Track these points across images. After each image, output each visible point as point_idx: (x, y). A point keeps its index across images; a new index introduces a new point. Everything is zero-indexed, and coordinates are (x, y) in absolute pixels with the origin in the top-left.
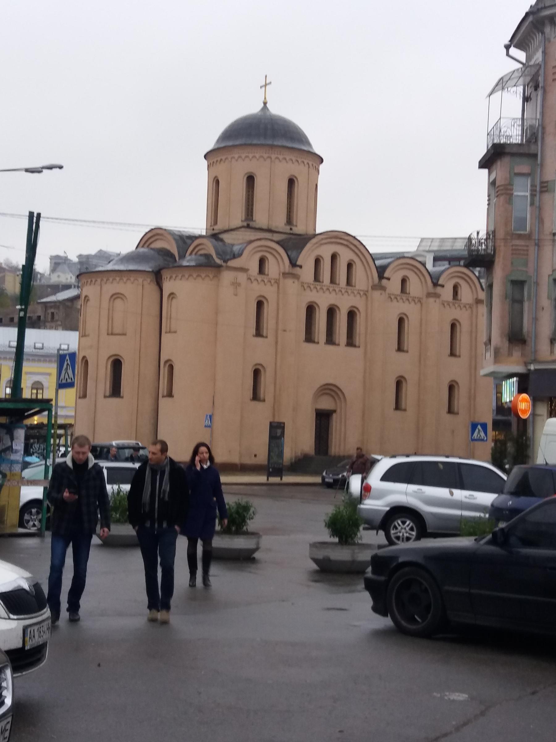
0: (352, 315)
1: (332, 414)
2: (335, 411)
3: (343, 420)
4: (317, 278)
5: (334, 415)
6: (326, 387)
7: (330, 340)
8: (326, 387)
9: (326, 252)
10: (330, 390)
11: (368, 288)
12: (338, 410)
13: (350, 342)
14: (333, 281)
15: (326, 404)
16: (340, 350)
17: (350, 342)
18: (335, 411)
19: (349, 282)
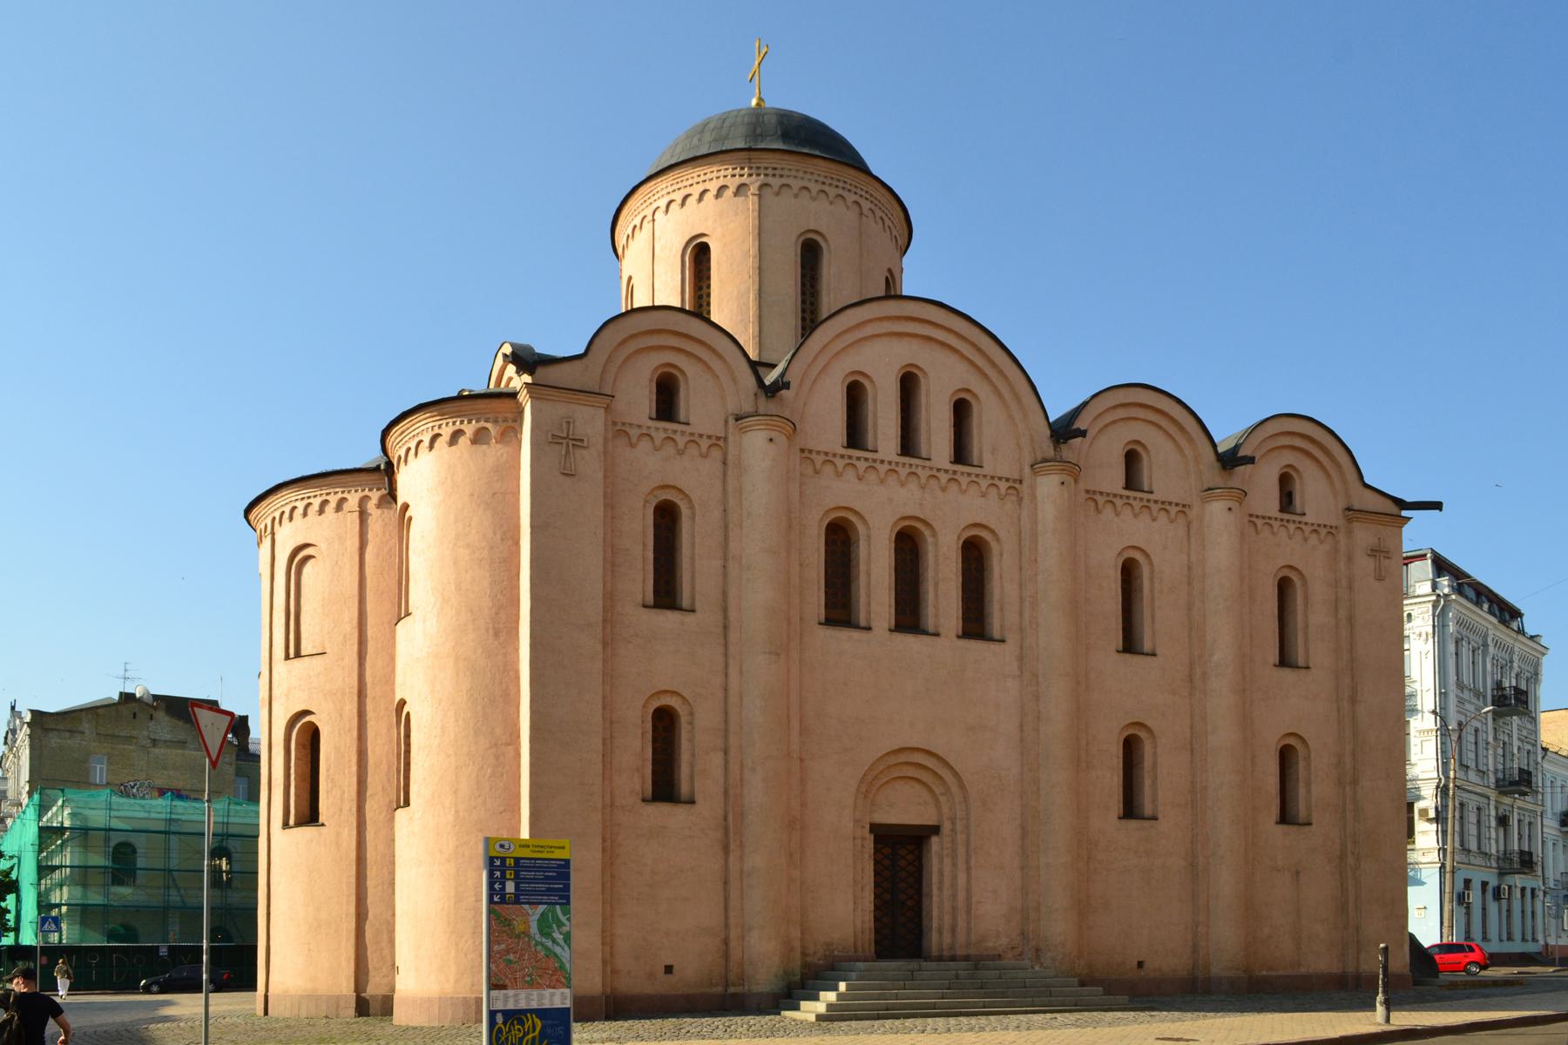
0: (974, 554)
1: (929, 837)
2: (935, 830)
3: (961, 850)
4: (855, 435)
5: (934, 839)
6: (903, 758)
7: (909, 618)
8: (903, 758)
9: (882, 366)
10: (914, 763)
11: (1021, 470)
12: (946, 827)
13: (975, 624)
14: (908, 445)
15: (905, 809)
16: (944, 647)
17: (975, 624)
18: (935, 830)
19: (961, 453)
